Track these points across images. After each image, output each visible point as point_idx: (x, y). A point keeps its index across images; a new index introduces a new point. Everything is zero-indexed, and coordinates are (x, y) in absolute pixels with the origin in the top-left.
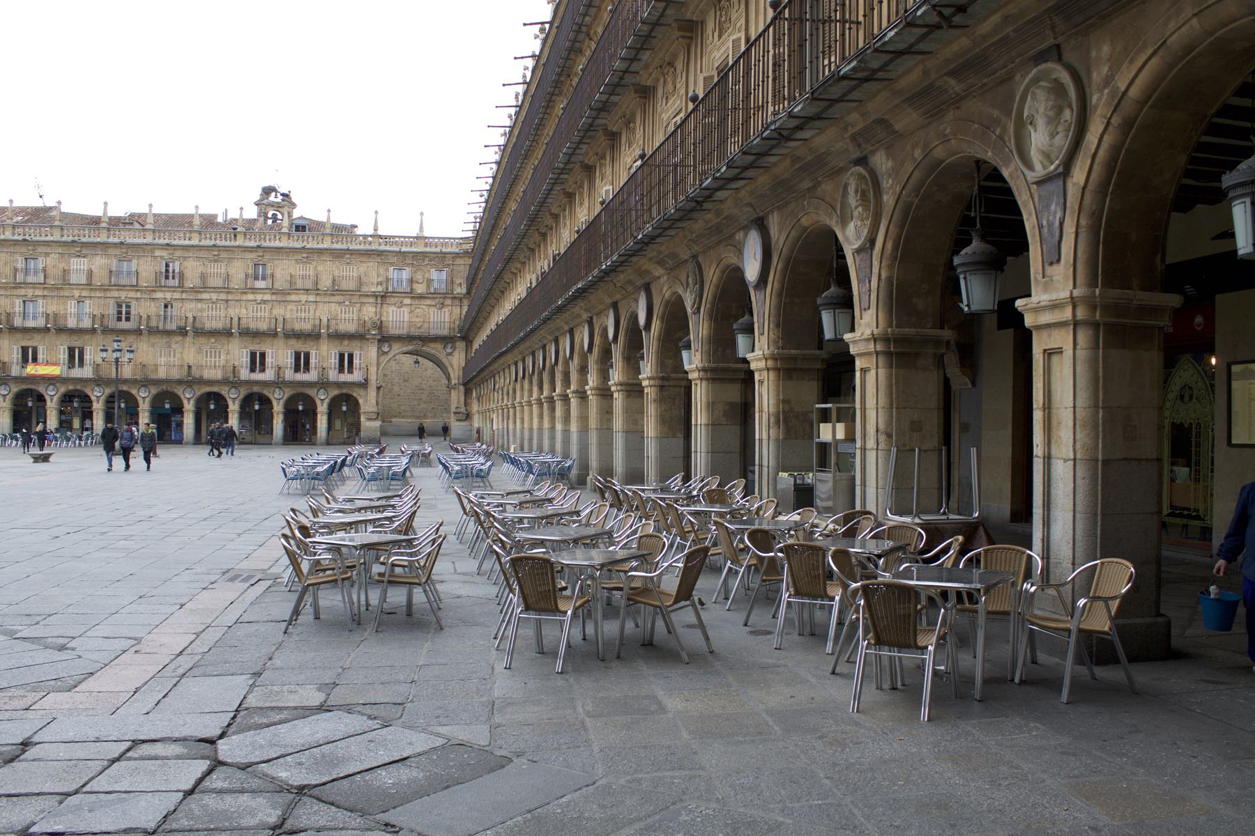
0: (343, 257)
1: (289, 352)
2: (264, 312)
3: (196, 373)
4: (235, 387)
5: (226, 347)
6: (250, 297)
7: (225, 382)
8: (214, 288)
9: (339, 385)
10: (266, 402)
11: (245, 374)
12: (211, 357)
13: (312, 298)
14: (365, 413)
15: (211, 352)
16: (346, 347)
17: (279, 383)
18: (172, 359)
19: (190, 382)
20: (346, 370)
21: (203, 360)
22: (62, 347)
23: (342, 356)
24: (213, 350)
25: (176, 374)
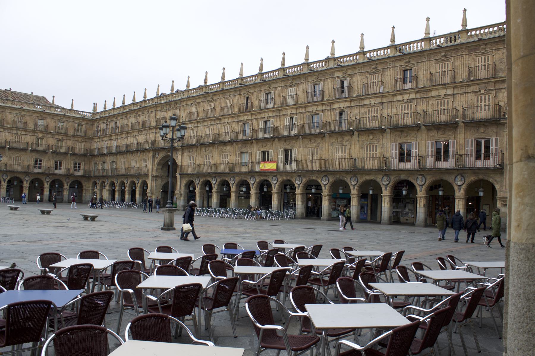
0: (478, 49)
1: (430, 142)
2: (410, 108)
3: (359, 164)
4: (387, 176)
5: (380, 142)
6: (399, 98)
7: (379, 171)
8: (372, 94)
9: (475, 171)
10: (411, 187)
11: (395, 164)
12: (370, 151)
13: (449, 92)
14: (501, 198)
15: (370, 146)
16: (482, 134)
17: (421, 171)
18: (343, 154)
19: (355, 172)
20: (483, 156)
21: (364, 154)
22: (280, 150)
23: (478, 144)
24: (372, 145)
25: (346, 166)
